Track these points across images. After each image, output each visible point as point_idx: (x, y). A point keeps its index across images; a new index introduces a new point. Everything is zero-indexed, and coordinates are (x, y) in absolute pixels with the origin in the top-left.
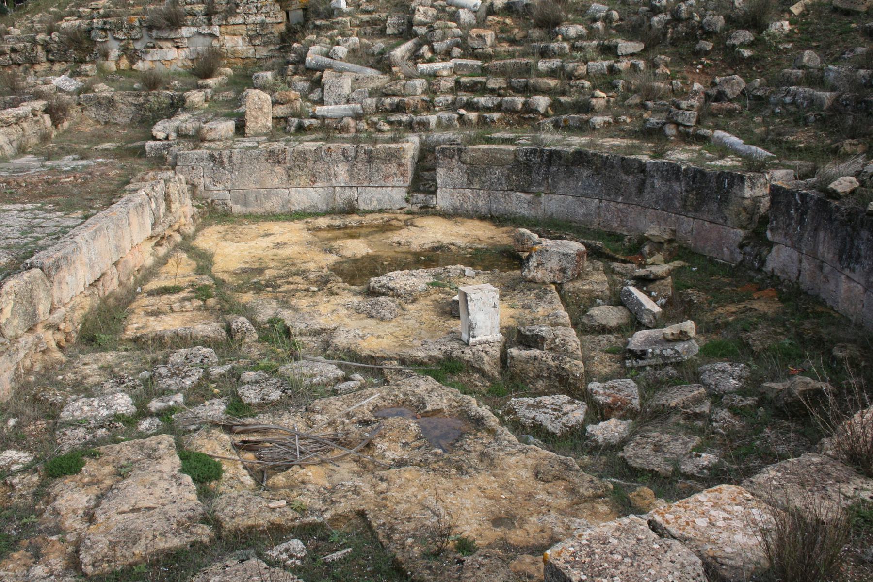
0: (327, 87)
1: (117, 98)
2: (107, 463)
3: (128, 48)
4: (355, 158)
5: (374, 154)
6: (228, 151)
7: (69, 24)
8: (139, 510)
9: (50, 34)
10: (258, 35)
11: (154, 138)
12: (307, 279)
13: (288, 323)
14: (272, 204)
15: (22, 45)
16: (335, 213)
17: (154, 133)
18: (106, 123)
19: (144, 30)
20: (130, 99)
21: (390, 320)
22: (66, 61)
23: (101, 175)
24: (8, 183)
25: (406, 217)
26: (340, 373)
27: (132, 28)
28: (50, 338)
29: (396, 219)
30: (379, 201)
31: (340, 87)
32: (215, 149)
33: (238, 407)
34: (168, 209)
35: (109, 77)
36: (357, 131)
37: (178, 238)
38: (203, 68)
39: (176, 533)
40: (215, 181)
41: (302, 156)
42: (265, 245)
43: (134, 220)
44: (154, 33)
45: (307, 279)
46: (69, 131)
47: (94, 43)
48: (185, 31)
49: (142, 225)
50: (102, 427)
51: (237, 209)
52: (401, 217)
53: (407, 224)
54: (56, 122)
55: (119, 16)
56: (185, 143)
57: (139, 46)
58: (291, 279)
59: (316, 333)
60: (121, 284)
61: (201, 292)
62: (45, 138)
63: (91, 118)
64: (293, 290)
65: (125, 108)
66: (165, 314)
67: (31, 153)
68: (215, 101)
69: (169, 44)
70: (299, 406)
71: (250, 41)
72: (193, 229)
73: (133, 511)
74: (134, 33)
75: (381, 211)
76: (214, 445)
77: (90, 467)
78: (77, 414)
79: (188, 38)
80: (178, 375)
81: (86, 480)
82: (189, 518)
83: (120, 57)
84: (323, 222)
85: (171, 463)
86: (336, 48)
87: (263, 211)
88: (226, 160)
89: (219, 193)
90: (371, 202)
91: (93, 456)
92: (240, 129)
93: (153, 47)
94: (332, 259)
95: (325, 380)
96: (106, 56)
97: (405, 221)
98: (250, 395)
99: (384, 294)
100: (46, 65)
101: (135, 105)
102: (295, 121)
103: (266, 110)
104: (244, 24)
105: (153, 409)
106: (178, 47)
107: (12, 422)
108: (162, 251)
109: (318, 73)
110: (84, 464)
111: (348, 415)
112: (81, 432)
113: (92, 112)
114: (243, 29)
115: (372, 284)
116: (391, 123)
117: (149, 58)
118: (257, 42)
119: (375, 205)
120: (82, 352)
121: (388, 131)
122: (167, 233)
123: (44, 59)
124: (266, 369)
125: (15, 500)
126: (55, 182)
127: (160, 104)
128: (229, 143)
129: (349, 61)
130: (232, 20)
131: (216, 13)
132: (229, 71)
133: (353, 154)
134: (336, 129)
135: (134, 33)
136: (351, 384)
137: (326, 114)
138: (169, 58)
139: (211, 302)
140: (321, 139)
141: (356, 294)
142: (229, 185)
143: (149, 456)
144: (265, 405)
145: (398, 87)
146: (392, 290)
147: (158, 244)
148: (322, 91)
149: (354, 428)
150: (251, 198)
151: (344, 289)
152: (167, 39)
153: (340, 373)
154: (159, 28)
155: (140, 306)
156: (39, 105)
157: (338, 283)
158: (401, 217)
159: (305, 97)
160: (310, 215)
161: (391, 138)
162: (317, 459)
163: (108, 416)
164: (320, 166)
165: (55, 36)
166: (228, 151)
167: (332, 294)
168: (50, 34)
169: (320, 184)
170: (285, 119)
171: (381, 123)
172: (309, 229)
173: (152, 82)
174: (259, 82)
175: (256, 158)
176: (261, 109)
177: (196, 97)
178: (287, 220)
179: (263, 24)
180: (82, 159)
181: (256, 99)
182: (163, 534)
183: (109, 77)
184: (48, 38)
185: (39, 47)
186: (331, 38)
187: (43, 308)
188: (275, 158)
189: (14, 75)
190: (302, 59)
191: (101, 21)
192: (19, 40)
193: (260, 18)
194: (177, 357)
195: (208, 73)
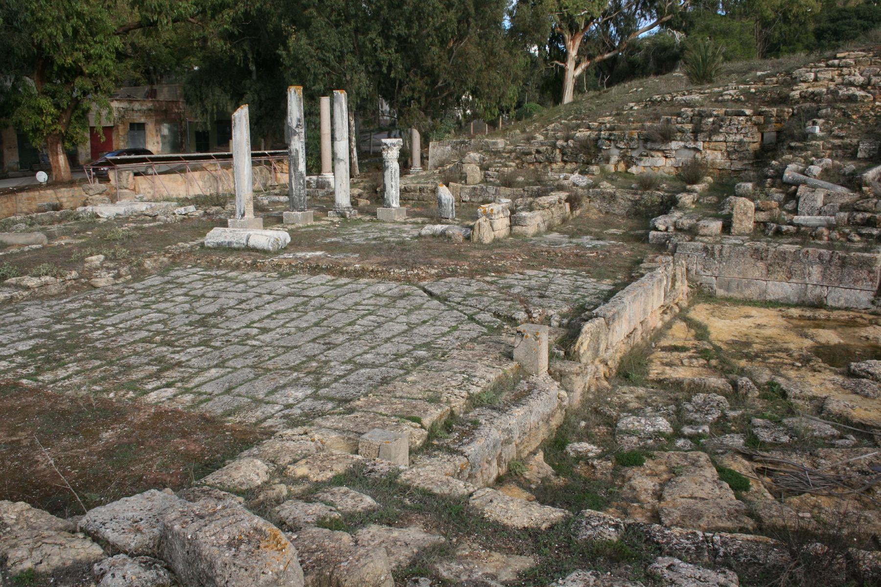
0: (802, 200)
1: (618, 194)
2: (661, 464)
3: (626, 156)
4: (830, 261)
5: (847, 260)
6: (719, 246)
7: (582, 134)
8: (696, 498)
9: (567, 141)
10: (735, 151)
11: (656, 229)
12: (790, 355)
13: (785, 388)
14: (751, 292)
15: (544, 148)
16: (805, 306)
17: (657, 225)
18: (607, 213)
19: (641, 142)
20: (628, 196)
21: (874, 398)
22: (576, 163)
23: (616, 254)
24: (549, 253)
25: (871, 317)
26: (836, 432)
27: (632, 139)
28: (602, 369)
29: (861, 317)
30: (847, 300)
31: (814, 200)
32: (707, 243)
33: (753, 441)
34: (673, 285)
35: (609, 177)
36: (830, 239)
37: (677, 310)
38: (689, 175)
39: (729, 519)
40: (705, 268)
41: (783, 256)
42: (748, 325)
43: (656, 292)
44: (649, 145)
45: (790, 355)
46: (580, 217)
47: (600, 149)
48: (674, 145)
49: (659, 296)
50: (650, 439)
51: (721, 292)
52: (865, 316)
53: (871, 323)
54: (572, 208)
55: (621, 129)
56: (681, 236)
57: (635, 154)
58: (776, 354)
59: (812, 398)
60: (642, 339)
61: (703, 354)
62: (564, 221)
63: (595, 208)
64: (779, 363)
65: (623, 202)
66: (677, 366)
67: (556, 231)
68: (700, 203)
69: (660, 154)
70: (804, 451)
71: (728, 156)
72: (686, 304)
73: (691, 498)
74: (633, 144)
75: (847, 309)
76: (740, 466)
77: (648, 463)
78: (630, 426)
79: (676, 150)
80: (701, 412)
81: (648, 472)
82: (736, 511)
83: (618, 161)
84: (795, 312)
85: (710, 472)
86: (812, 167)
87: (742, 296)
88: (717, 253)
89: (707, 278)
90: (839, 300)
91: (650, 457)
92: (727, 228)
93: (647, 156)
94: (808, 343)
95: (823, 435)
96: (607, 160)
97: (870, 320)
98: (765, 436)
99: (863, 377)
100: (560, 164)
101: (632, 201)
102: (774, 226)
103: (749, 215)
104: (725, 141)
105: (686, 433)
106: (666, 157)
107: (583, 424)
108: (667, 318)
109: (793, 188)
110: (644, 461)
111: (848, 464)
112: (635, 439)
113: (597, 204)
114: (723, 146)
115: (852, 367)
116: (861, 235)
117: (642, 164)
118: (734, 157)
119: (842, 303)
120: (620, 384)
121: (858, 241)
122: (672, 305)
123: (560, 160)
124: (771, 419)
125: (598, 475)
126: (582, 256)
127: (652, 202)
128: (718, 239)
129: (822, 179)
130: (714, 138)
131: (703, 131)
132: (710, 179)
133: (827, 258)
134: (811, 235)
135: (633, 144)
136: (847, 442)
137: (802, 222)
138: (658, 165)
139: (713, 362)
140: (797, 243)
141: (836, 373)
142: (716, 273)
143: (693, 464)
144: (776, 445)
145: (870, 204)
146: (872, 374)
147: (664, 312)
148: (797, 203)
149: (856, 475)
150: (734, 285)
151: (825, 368)
152: (658, 150)
153: (836, 432)
154: (654, 141)
155: (656, 358)
156: (564, 195)
157: (818, 363)
158: (865, 316)
159: (781, 206)
160: (782, 305)
161: (862, 248)
162: (825, 492)
163: (654, 432)
164: (796, 265)
165: (571, 143)
166: (719, 246)
167: (815, 371)
168: (567, 141)
169: (794, 281)
170: (765, 224)
171: (853, 234)
172: (783, 317)
173: (647, 183)
174: (740, 191)
175: (743, 254)
176: (746, 214)
177: (686, 199)
178: (762, 306)
179: (741, 142)
180: (598, 239)
181: (742, 205)
182: (720, 517)
183: (609, 177)
184: (565, 144)
185: (558, 151)
186: (805, 158)
187: (602, 347)
188: (758, 255)
189: (536, 170)
190: (780, 173)
191: (607, 133)
192: (542, 144)
193: (738, 137)
194: (699, 398)
195: (695, 180)
